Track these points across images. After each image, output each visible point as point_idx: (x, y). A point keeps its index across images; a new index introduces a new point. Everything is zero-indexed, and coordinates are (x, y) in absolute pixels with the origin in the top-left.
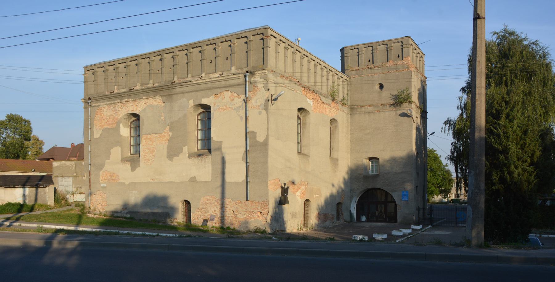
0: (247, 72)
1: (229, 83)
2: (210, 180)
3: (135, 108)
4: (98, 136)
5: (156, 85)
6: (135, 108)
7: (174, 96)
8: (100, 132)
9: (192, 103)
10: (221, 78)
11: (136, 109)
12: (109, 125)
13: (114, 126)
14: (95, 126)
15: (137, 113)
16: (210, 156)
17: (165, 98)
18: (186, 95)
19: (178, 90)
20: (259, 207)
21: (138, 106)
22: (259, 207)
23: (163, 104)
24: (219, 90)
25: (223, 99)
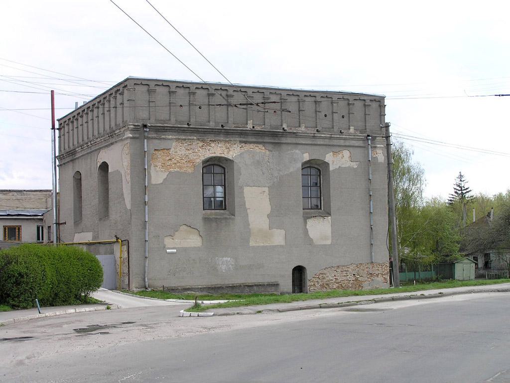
0: (368, 136)
1: (347, 143)
2: (330, 243)
3: (226, 151)
4: (162, 182)
5: (258, 128)
6: (226, 151)
7: (284, 147)
8: (165, 177)
9: (306, 157)
10: (341, 136)
11: (228, 153)
12: (180, 167)
13: (190, 170)
14: (152, 167)
15: (230, 157)
16: (330, 217)
17: (270, 147)
18: (300, 147)
19: (289, 140)
20: (380, 269)
21: (232, 151)
22: (380, 269)
23: (268, 152)
24: (337, 149)
25: (342, 158)
